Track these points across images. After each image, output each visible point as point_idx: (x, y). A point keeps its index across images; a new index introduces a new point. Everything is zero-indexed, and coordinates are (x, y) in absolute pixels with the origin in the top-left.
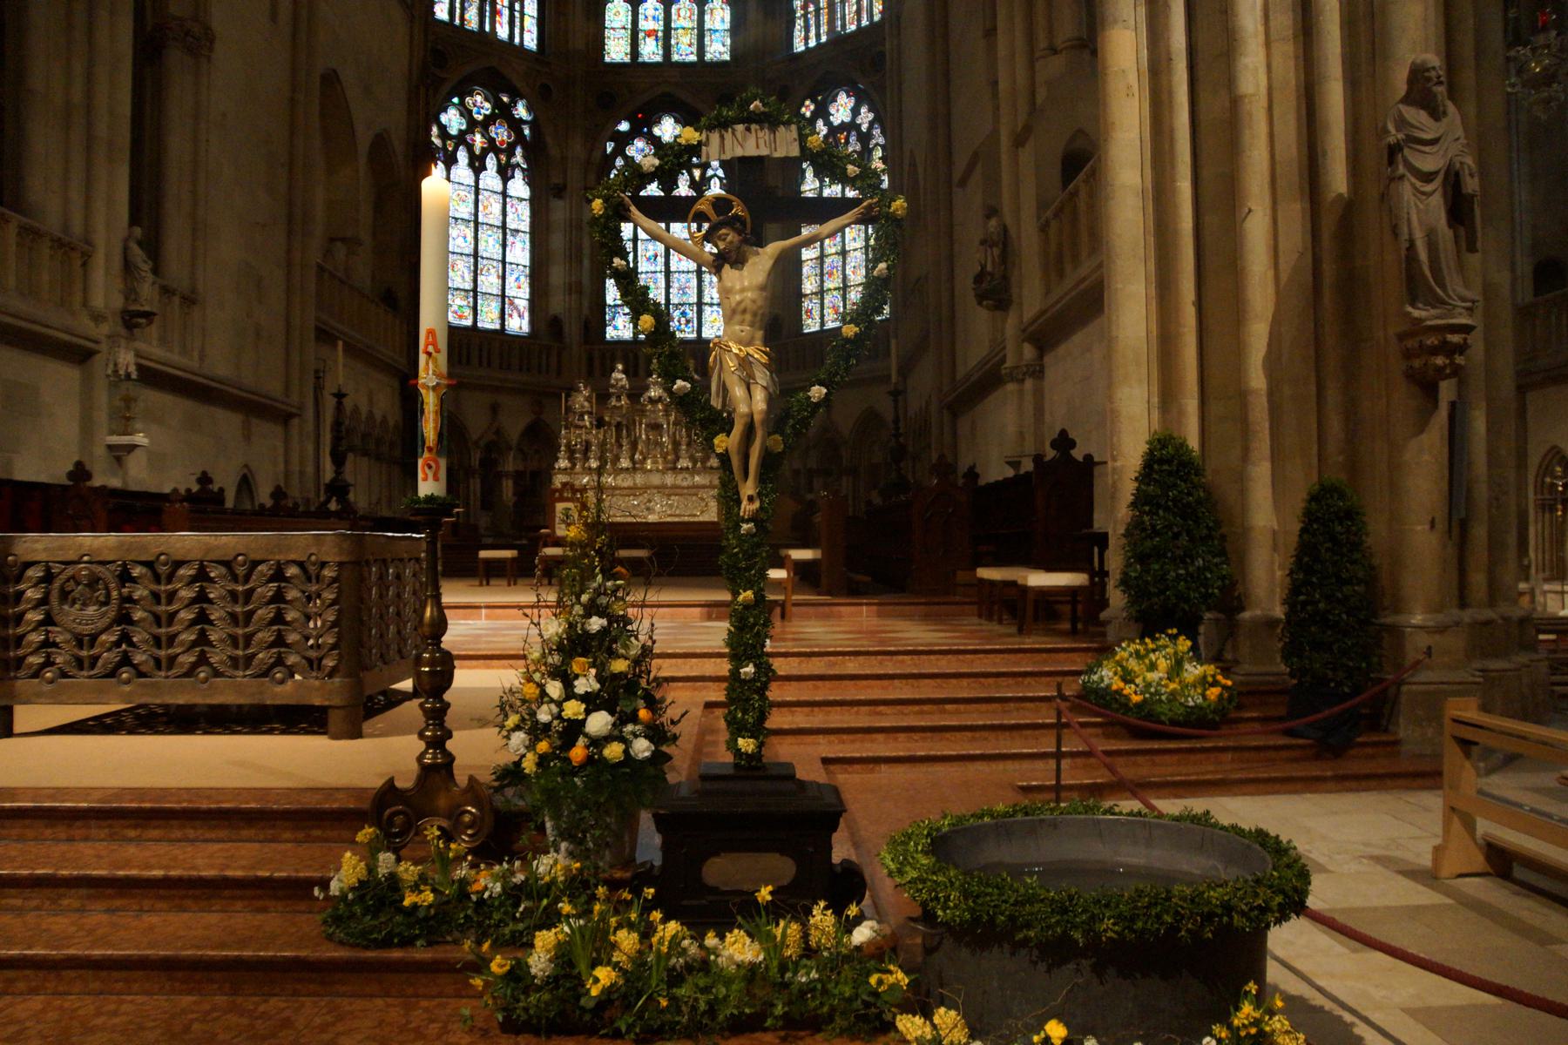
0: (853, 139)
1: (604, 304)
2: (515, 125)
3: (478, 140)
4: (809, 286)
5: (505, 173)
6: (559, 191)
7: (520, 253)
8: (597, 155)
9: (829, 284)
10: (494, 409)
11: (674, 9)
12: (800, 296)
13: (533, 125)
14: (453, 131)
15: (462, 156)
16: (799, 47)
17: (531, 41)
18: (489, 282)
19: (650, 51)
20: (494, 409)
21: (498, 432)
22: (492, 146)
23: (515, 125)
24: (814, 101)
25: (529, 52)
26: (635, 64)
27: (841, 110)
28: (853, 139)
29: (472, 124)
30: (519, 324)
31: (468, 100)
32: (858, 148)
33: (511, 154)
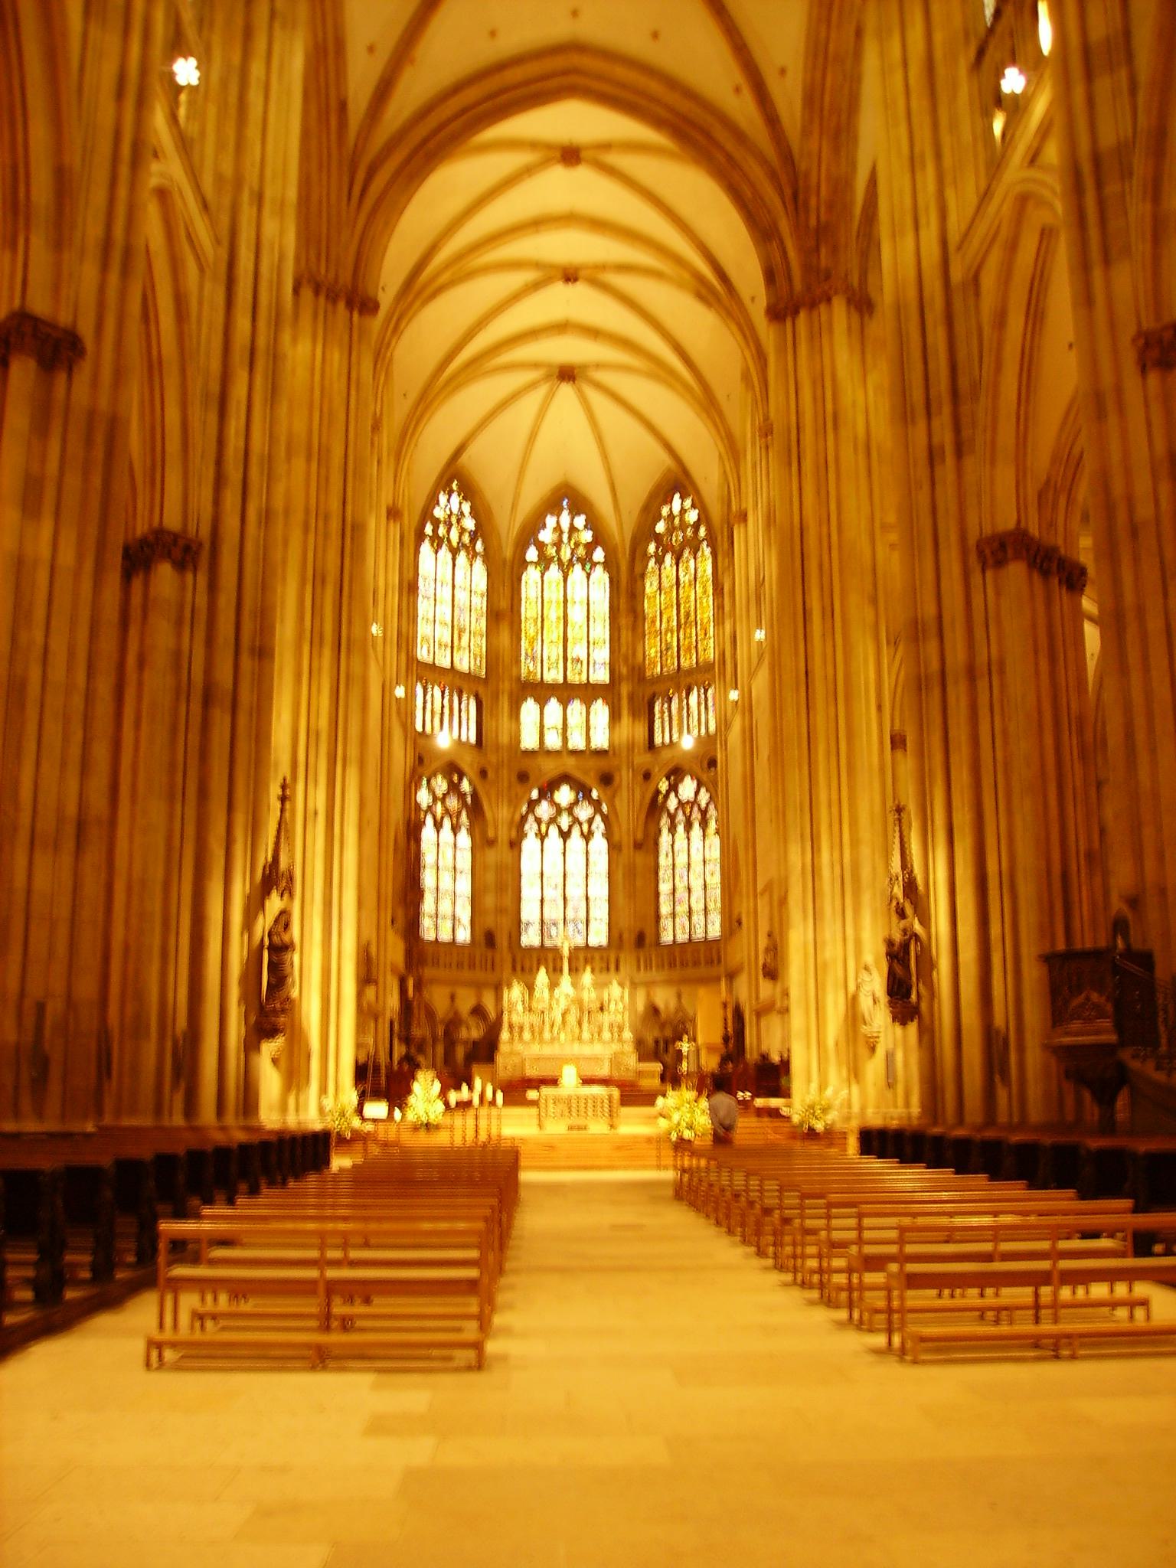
0: (696, 809)
1: (519, 921)
2: (462, 796)
3: (439, 809)
4: (665, 909)
5: (455, 829)
6: (491, 843)
7: (464, 886)
8: (517, 817)
9: (678, 909)
10: (453, 998)
11: (569, 708)
12: (658, 917)
13: (475, 795)
14: (424, 806)
15: (429, 820)
16: (658, 740)
17: (473, 739)
18: (445, 907)
19: (553, 742)
20: (453, 998)
21: (456, 1013)
22: (447, 811)
23: (462, 796)
24: (668, 778)
25: (471, 746)
26: (543, 751)
27: (687, 788)
28: (696, 809)
29: (435, 799)
30: (464, 935)
31: (433, 782)
32: (699, 816)
33: (459, 814)
